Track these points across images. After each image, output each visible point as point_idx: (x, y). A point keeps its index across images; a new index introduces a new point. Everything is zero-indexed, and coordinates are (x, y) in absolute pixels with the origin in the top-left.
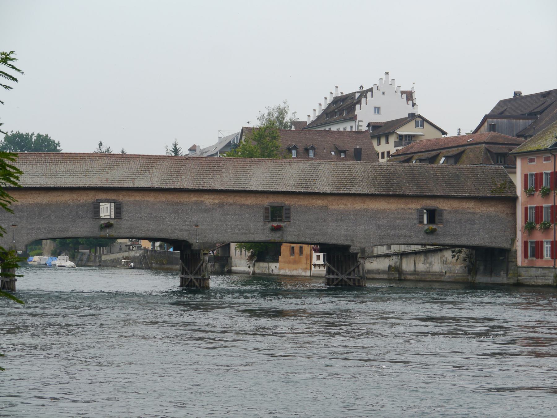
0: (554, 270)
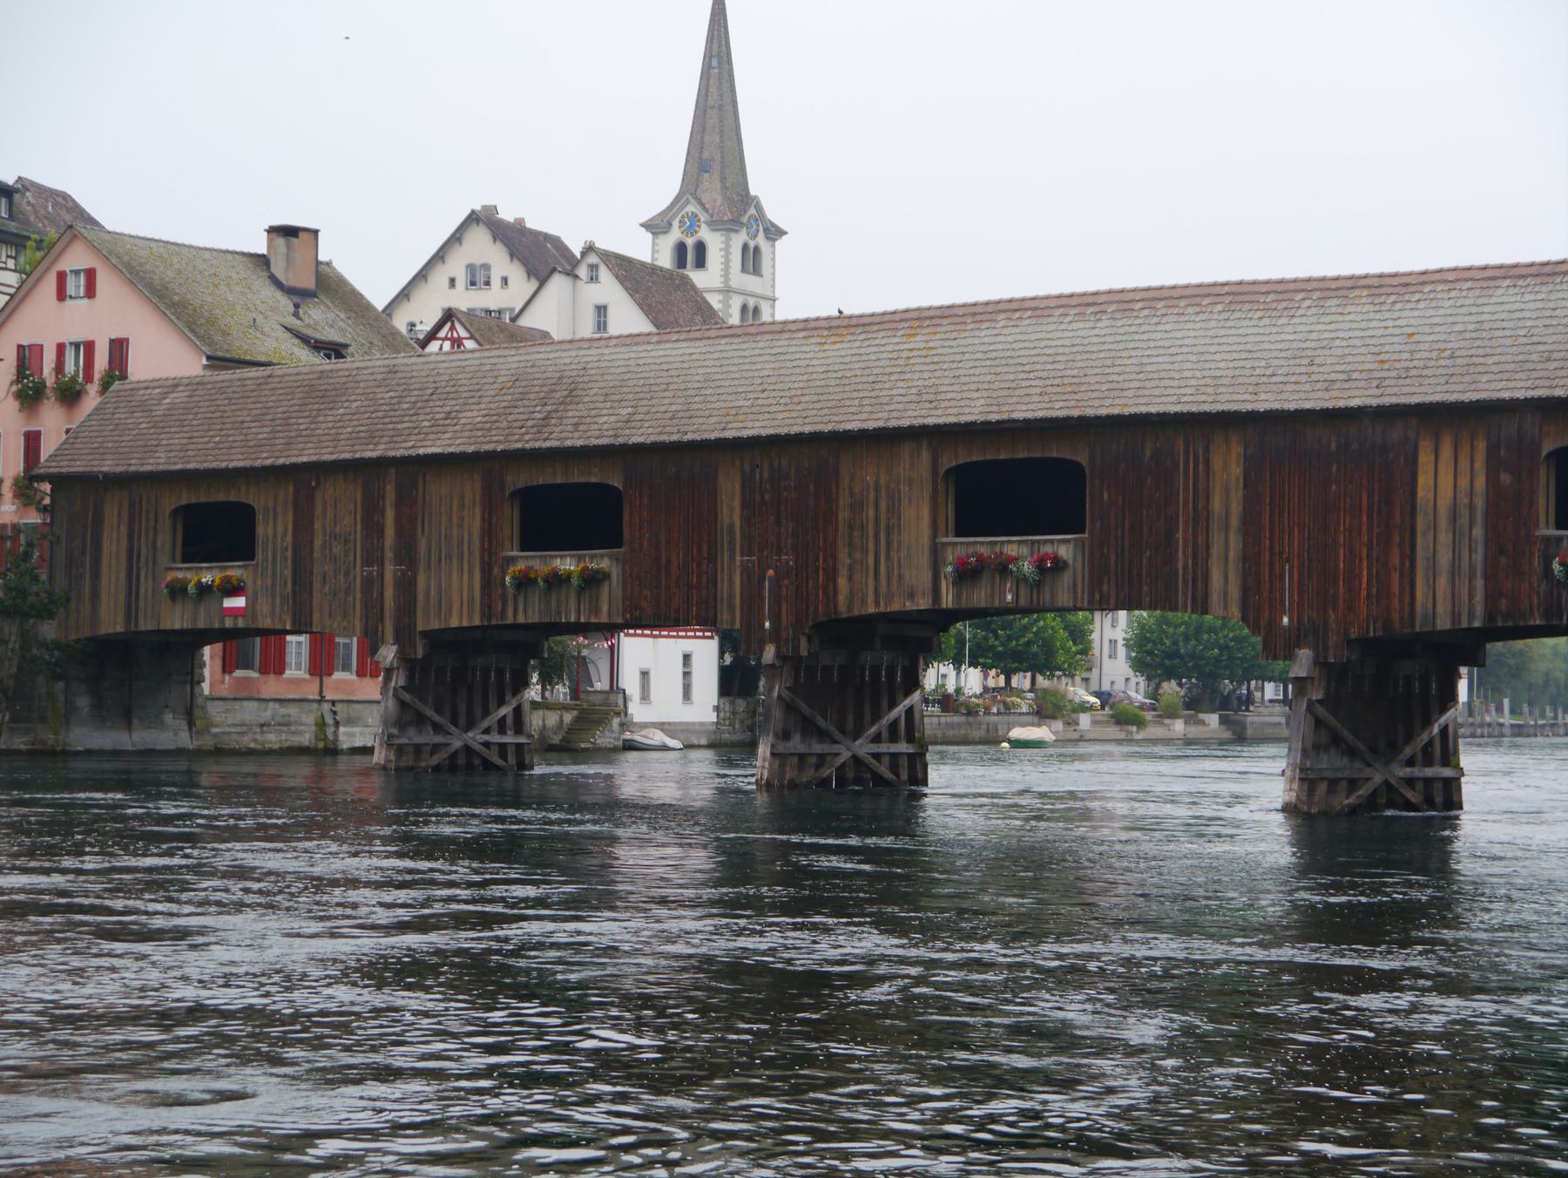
0: (315, 706)
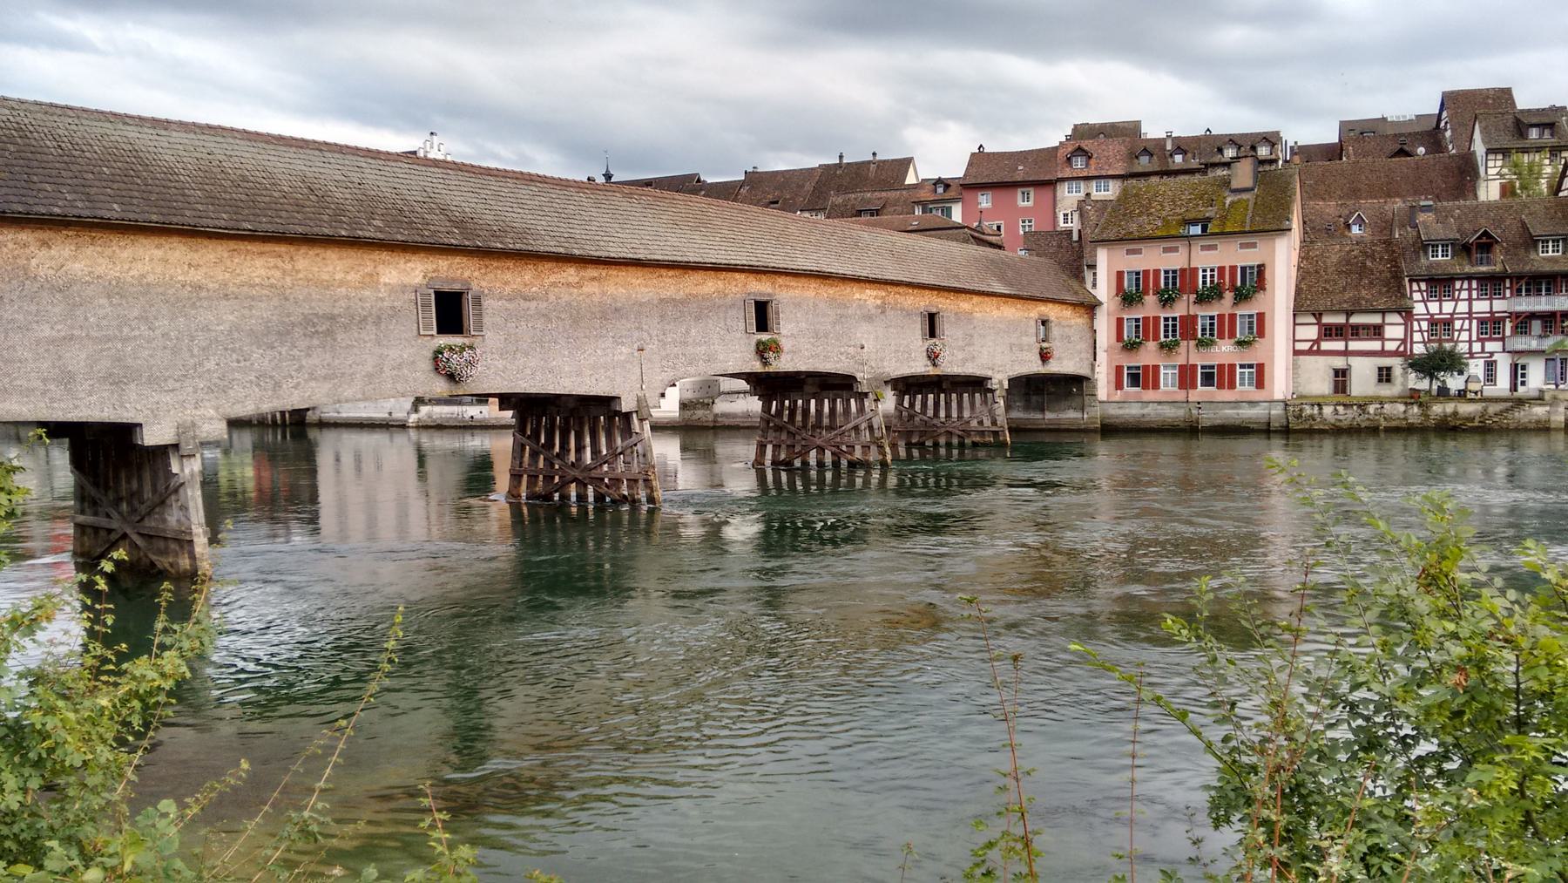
0: (1185, 405)
